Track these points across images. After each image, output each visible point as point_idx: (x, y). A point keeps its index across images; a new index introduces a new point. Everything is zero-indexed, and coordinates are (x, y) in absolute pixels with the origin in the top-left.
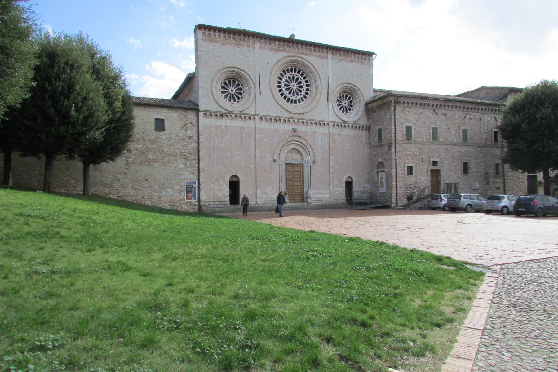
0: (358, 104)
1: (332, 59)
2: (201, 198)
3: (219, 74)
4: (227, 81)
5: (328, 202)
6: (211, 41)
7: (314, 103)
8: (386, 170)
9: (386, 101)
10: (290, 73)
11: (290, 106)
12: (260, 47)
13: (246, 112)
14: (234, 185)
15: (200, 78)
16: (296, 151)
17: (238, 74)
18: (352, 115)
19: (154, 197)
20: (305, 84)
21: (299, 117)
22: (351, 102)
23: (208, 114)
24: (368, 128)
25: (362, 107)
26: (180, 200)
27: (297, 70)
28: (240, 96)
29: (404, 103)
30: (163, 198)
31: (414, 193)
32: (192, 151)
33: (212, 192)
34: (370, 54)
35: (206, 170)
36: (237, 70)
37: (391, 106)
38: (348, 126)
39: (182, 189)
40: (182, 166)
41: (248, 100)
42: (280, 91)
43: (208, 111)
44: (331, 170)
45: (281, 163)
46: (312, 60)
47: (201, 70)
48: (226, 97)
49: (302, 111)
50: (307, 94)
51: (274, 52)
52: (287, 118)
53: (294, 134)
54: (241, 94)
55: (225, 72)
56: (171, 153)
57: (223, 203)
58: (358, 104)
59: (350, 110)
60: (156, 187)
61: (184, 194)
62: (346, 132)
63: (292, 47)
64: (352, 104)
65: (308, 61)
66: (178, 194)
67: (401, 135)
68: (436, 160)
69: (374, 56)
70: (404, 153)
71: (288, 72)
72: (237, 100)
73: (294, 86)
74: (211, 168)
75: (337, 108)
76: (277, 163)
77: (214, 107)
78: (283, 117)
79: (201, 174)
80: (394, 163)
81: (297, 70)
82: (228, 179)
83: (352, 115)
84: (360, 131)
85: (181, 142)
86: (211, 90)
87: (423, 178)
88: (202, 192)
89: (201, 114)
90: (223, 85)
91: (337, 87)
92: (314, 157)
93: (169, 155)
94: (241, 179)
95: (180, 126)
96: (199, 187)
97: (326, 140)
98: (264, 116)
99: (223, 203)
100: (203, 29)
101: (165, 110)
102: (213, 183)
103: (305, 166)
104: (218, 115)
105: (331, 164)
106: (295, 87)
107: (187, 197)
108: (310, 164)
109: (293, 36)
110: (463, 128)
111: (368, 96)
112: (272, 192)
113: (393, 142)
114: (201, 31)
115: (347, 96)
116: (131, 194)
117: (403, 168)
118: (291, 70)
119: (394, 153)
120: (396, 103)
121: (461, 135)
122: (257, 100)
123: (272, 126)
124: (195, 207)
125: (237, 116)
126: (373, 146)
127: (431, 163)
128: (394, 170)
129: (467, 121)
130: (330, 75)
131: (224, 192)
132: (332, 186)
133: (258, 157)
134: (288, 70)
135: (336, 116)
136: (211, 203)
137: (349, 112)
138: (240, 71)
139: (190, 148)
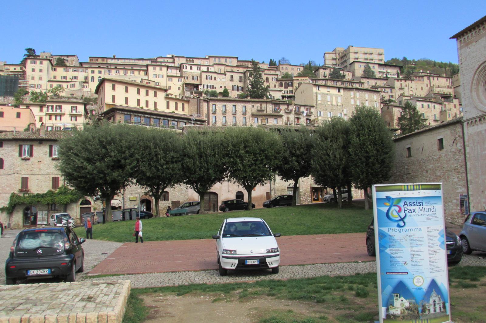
3: (476, 76)
35: (473, 181)
40: (456, 180)
56: (449, 169)
74: (477, 179)
89: (465, 124)
101: (442, 130)
102: (480, 196)
139: (460, 161)
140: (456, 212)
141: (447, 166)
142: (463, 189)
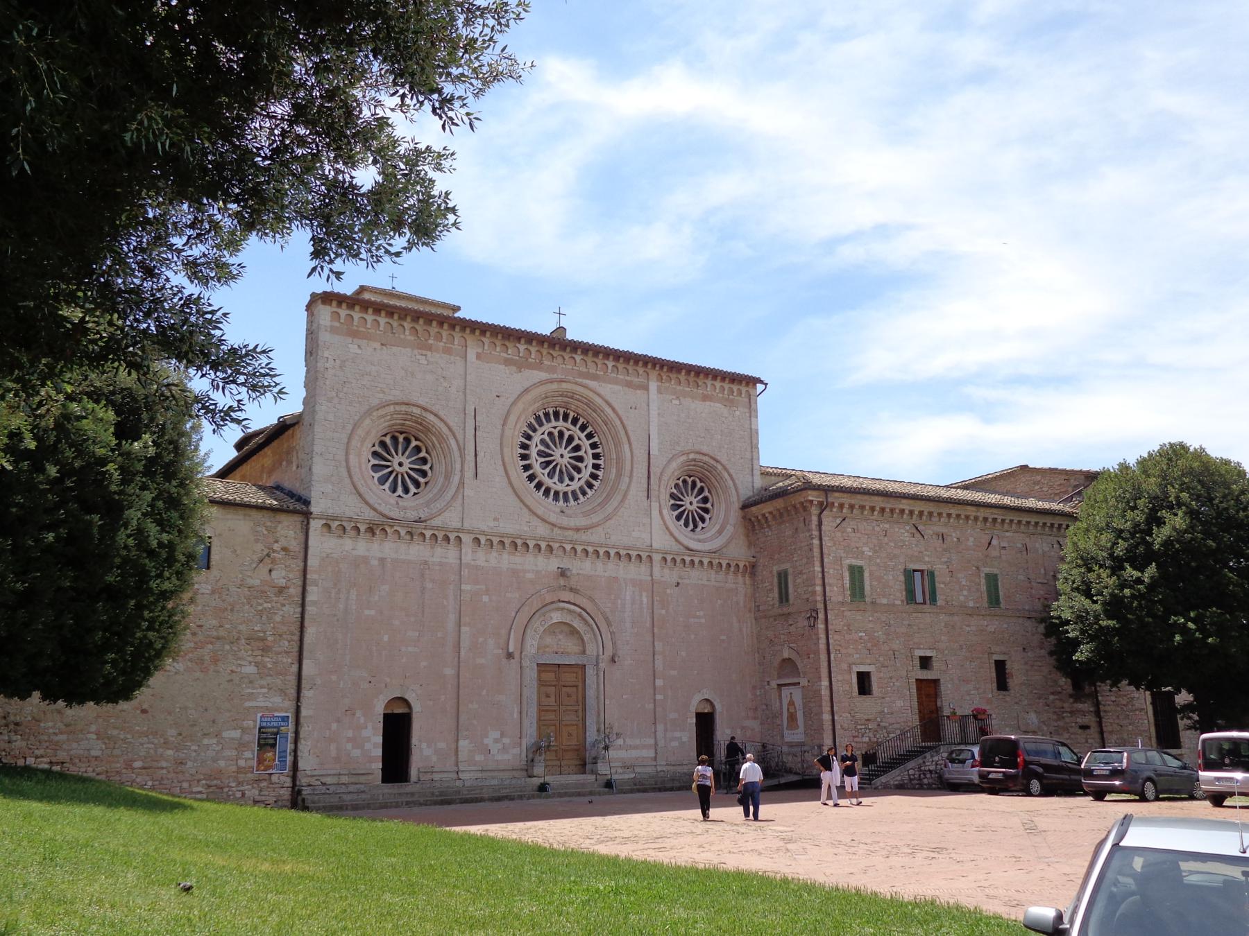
0: (723, 506)
1: (659, 391)
2: (301, 765)
3: (367, 421)
4: (388, 440)
5: (650, 770)
6: (354, 334)
7: (614, 503)
8: (804, 682)
9: (799, 498)
10: (554, 423)
11: (549, 507)
12: (479, 356)
13: (437, 522)
14: (397, 729)
15: (318, 429)
16: (566, 629)
17: (420, 422)
18: (709, 534)
19: (164, 764)
20: (590, 452)
21: (576, 536)
22: (705, 500)
23: (335, 524)
24: (752, 569)
25: (735, 514)
26: (240, 770)
27: (572, 415)
28: (422, 480)
29: (841, 506)
30: (190, 764)
31: (879, 744)
32: (285, 629)
33: (333, 747)
34: (752, 381)
35: (319, 681)
36: (416, 411)
37: (810, 514)
38: (701, 562)
39: (247, 738)
40: (251, 669)
41: (442, 491)
42: (526, 468)
43: (335, 518)
44: (659, 682)
45: (526, 663)
46: (611, 393)
47: (322, 408)
48: (382, 481)
49: (581, 522)
50: (594, 476)
51: (514, 368)
52: (544, 539)
53: (562, 582)
54: (424, 474)
55: (383, 416)
56: (222, 633)
57: (362, 779)
58: (723, 506)
59: (703, 520)
60: (172, 732)
61: (251, 754)
62: (695, 577)
63: (560, 360)
64: (709, 505)
65: (599, 395)
66: (234, 753)
67: (838, 589)
68: (928, 653)
69: (760, 387)
70: (847, 637)
71: (549, 421)
72: (413, 489)
73: (562, 456)
74: (334, 678)
75: (670, 516)
76: (514, 663)
77: (350, 507)
78: (534, 538)
79: (307, 694)
80: (824, 664)
81: (572, 415)
82: (379, 709)
83: (709, 534)
84: (731, 577)
85: (254, 602)
86: (347, 461)
87: (899, 703)
88: (304, 747)
89: (315, 525)
90: (377, 448)
91: (669, 462)
92: (614, 644)
93: (218, 638)
94: (417, 708)
95: (256, 558)
96: (297, 733)
97: (645, 600)
98: (483, 533)
99: (362, 779)
100: (334, 303)
102: (338, 721)
103: (590, 672)
104: (363, 528)
105: (659, 664)
106: (566, 460)
107: (260, 762)
108: (602, 665)
109: (561, 329)
110: (987, 570)
111: (748, 485)
112: (499, 746)
113: (820, 606)
114: (328, 307)
115: (694, 483)
116: (94, 753)
117: (847, 677)
118: (556, 414)
119: (822, 636)
120: (823, 507)
121: (984, 588)
122: (468, 492)
123: (505, 560)
124: (282, 792)
125: (415, 530)
126: (765, 617)
127: (917, 661)
128: (825, 683)
129: (995, 553)
130: (655, 427)
131: (368, 746)
132: (660, 727)
133: (465, 643)
134: (547, 415)
135: (668, 537)
136: (329, 780)
137: (701, 525)
138: (424, 414)
139: (278, 618)
140: (234, 768)
141: (214, 622)
142: (277, 700)
